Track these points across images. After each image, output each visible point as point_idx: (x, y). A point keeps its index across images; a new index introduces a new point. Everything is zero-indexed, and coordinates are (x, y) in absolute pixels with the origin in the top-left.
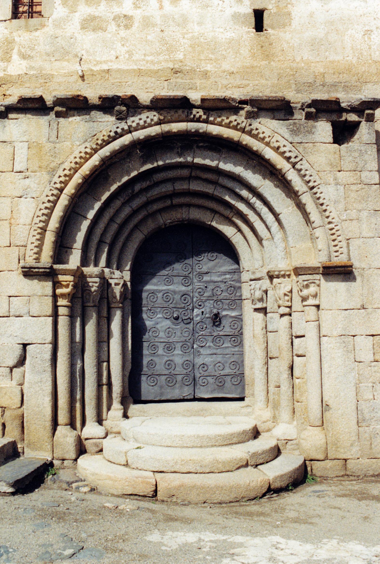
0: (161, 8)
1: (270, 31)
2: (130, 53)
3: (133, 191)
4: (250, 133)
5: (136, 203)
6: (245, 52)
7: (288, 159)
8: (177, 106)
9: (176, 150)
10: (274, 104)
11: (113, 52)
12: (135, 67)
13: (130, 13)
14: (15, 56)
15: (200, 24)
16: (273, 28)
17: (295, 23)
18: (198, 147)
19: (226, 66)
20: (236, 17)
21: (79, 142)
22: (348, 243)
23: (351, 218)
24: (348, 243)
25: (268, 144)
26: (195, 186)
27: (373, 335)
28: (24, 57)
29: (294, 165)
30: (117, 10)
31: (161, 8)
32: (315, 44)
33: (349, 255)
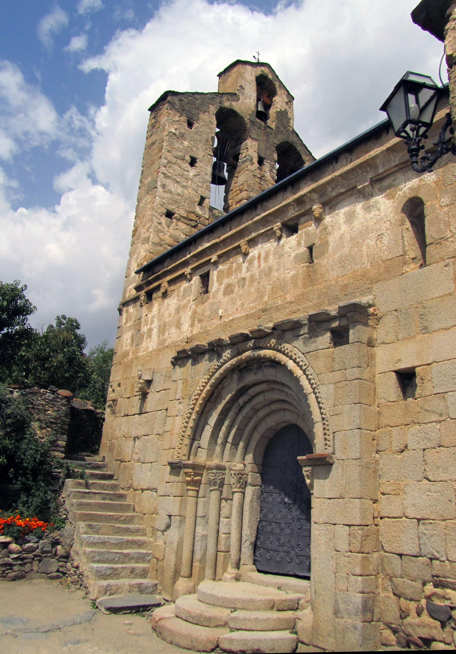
0: (259, 266)
1: (315, 261)
2: (242, 304)
3: (239, 404)
4: (280, 351)
5: (244, 412)
6: (300, 283)
7: (301, 367)
8: (238, 342)
9: (254, 371)
10: (289, 326)
11: (235, 307)
12: (244, 314)
13: (245, 276)
14: (196, 322)
15: (278, 270)
16: (317, 259)
17: (330, 248)
18: (265, 366)
19: (289, 298)
21: (202, 375)
22: (334, 436)
23: (336, 413)
24: (334, 436)
25: (291, 358)
26: (276, 396)
27: (349, 526)
28: (200, 321)
29: (304, 372)
31: (259, 266)
32: (343, 262)
33: (334, 448)
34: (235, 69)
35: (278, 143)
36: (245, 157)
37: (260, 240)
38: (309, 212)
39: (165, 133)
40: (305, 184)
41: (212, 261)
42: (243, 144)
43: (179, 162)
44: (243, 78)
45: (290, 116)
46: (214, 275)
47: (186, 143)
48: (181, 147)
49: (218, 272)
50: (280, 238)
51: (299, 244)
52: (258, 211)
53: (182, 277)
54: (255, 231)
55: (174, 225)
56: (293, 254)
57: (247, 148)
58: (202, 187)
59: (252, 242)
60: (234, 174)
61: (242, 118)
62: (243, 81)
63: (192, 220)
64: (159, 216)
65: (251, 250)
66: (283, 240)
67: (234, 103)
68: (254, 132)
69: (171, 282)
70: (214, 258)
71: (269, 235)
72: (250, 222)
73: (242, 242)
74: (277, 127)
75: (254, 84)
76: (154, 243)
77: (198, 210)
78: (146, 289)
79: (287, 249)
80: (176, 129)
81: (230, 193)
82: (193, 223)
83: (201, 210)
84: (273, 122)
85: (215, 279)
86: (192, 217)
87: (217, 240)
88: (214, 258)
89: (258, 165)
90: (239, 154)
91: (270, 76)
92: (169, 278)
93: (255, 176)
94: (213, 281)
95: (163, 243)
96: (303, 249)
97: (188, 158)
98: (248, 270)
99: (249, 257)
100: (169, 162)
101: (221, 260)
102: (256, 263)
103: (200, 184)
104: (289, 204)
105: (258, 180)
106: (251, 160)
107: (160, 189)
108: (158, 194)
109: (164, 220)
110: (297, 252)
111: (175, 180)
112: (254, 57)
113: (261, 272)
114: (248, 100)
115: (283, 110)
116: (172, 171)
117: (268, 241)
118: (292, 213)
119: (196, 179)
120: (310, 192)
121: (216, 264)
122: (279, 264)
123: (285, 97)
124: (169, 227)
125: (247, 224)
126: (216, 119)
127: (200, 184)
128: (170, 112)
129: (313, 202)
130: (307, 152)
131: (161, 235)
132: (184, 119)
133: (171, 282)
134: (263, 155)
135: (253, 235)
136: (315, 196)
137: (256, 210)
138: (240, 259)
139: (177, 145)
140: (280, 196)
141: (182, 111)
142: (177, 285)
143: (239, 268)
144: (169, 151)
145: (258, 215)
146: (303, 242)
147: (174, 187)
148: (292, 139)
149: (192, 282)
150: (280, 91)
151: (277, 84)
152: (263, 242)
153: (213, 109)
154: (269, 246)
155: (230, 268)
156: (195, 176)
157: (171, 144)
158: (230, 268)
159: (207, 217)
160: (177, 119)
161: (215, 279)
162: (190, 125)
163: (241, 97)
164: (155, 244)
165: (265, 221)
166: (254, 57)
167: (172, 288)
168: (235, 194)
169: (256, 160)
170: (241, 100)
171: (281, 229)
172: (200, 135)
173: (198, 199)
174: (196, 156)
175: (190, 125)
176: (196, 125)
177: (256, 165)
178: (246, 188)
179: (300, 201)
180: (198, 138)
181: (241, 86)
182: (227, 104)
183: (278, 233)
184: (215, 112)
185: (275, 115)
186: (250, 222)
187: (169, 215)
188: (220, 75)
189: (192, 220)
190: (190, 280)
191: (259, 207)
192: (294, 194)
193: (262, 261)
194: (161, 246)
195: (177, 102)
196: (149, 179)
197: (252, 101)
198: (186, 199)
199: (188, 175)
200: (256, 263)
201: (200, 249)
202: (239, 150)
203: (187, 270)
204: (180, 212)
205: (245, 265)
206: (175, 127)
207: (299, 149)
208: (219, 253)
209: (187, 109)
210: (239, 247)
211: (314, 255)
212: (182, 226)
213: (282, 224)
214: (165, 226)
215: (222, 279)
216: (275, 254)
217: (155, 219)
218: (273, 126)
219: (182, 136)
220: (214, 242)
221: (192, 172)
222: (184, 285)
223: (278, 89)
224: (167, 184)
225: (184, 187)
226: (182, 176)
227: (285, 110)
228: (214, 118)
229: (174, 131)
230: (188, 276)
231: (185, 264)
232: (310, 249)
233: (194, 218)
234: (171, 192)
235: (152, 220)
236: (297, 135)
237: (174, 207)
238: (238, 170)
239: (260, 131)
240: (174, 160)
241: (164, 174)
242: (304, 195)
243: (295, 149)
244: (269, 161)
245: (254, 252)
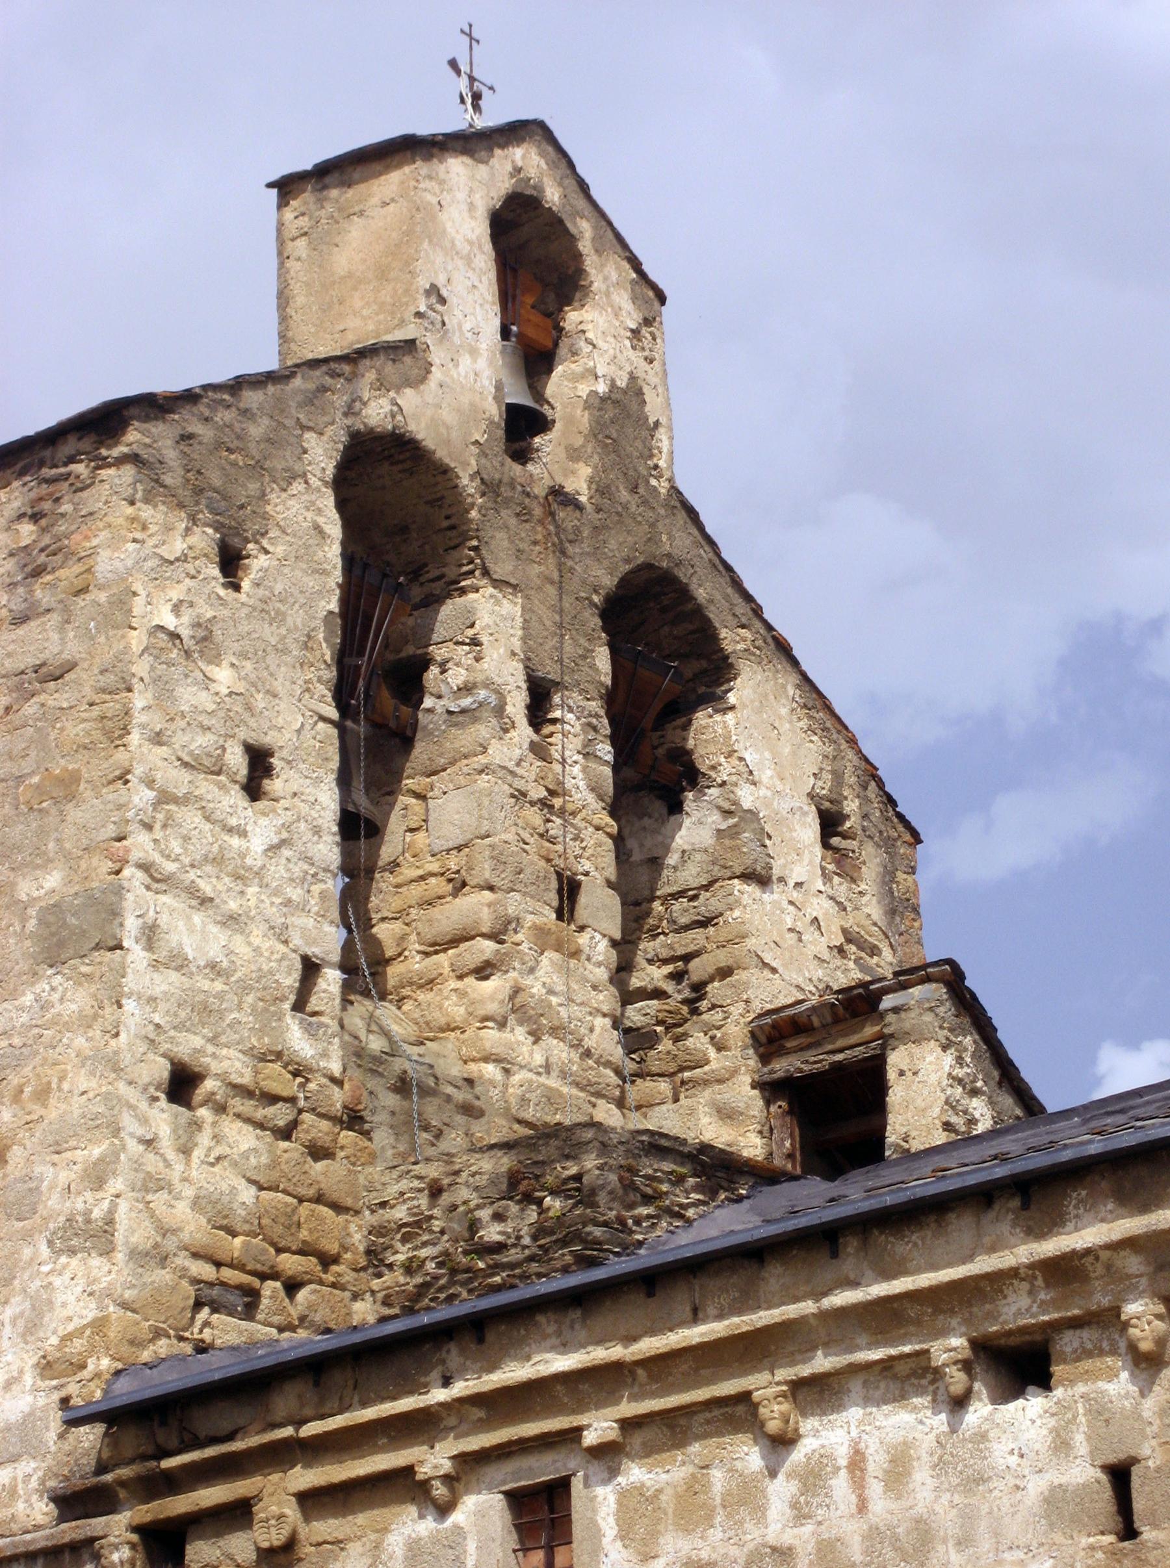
0: (862, 1506)
1: (1148, 1534)
13: (787, 1538)
16: (1155, 1526)
20: (1054, 1500)
30: (753, 1535)
31: (862, 1506)
34: (391, 182)
35: (609, 582)
36: (467, 689)
37: (856, 1386)
38: (1108, 1320)
39: (137, 640)
40: (1090, 1205)
41: (590, 1438)
42: (448, 609)
43: (205, 787)
44: (436, 236)
45: (653, 408)
46: (598, 1504)
47: (223, 676)
48: (205, 700)
49: (623, 1495)
50: (959, 1403)
51: (1061, 1445)
52: (848, 1265)
53: (402, 1485)
54: (829, 1345)
55: (204, 1139)
56: (1036, 1486)
57: (475, 642)
58: (303, 908)
59: (817, 1393)
60: (398, 776)
61: (445, 471)
62: (439, 258)
63: (272, 1099)
64: (143, 1105)
65: (808, 1425)
66: (979, 1411)
67: (409, 399)
68: (502, 541)
69: (313, 1501)
70: (599, 1427)
71: (907, 1377)
72: (808, 1307)
73: (765, 1385)
74: (602, 490)
75: (485, 260)
76: (139, 1256)
77: (297, 1040)
78: (146, 1512)
79: (1000, 1452)
80: (176, 609)
81: (383, 882)
82: (280, 1115)
83: (310, 1031)
84: (574, 455)
85: (608, 1525)
86: (277, 1079)
87: (616, 1352)
88: (599, 1427)
89: (529, 731)
90: (425, 663)
91: (553, 195)
92: (304, 1477)
93: (520, 795)
94: (597, 1534)
95: (171, 1244)
96: (1083, 1472)
97: (237, 760)
98: (800, 1514)
99: (798, 1455)
100: (165, 798)
101: (637, 1440)
102: (840, 1485)
103: (295, 894)
104: (1013, 1273)
105: (534, 816)
106: (500, 710)
107: (137, 955)
108: (130, 982)
109: (164, 1118)
110: (1054, 1477)
111: (192, 891)
112: (453, 64)
113: (873, 1535)
114: (465, 361)
115: (622, 383)
116: (176, 846)
117: (900, 1397)
118: (1020, 1311)
119: (277, 871)
120: (1114, 1247)
121: (608, 1455)
122: (968, 1517)
123: (623, 299)
124: (186, 1151)
125: (792, 1311)
126: (341, 505)
127: (295, 894)
128: (146, 512)
129: (1125, 1286)
130: (742, 608)
131: (159, 1199)
132: (205, 539)
133: (313, 1501)
134: (549, 670)
135: (822, 1362)
136: (1133, 1263)
137: (835, 1254)
138: (750, 1456)
139: (190, 696)
140: (961, 1226)
141: (194, 496)
142: (361, 1519)
143: (747, 1498)
144: (158, 739)
145: (854, 1284)
146: (1080, 1442)
147: (191, 930)
148: (675, 542)
149: (458, 1517)
150: (604, 274)
151: (584, 230)
152: (867, 1401)
153: (322, 455)
154: (912, 1422)
155: (695, 1487)
156: (273, 849)
157: (164, 692)
158: (695, 1487)
159: (335, 1068)
160: (178, 546)
161: (608, 1525)
162: (231, 562)
163: (437, 356)
164: (139, 1256)
165: (884, 1317)
166: (453, 64)
167: (326, 1527)
168: (416, 892)
169: (517, 704)
170: (436, 374)
171: (966, 1366)
172: (279, 618)
173: (291, 980)
174: (269, 740)
175: (231, 562)
176: (257, 564)
177: (524, 732)
178: (485, 871)
179: (1063, 1271)
180: (270, 633)
181: (433, 291)
182: (377, 413)
183: (957, 1379)
184: (330, 471)
185: (584, 420)
186: (808, 1307)
187: (182, 1084)
188: (287, 187)
189: (272, 1099)
190: (444, 1510)
191: (851, 1245)
192: (1038, 1232)
193: (875, 1488)
194: (163, 1260)
195: (171, 454)
196: (53, 880)
197: (482, 364)
198: (244, 988)
199: (243, 855)
200: (840, 1485)
201: (513, 1373)
202: (424, 636)
203: (434, 1459)
204: (226, 1064)
205: (781, 1492)
206: (176, 593)
207: (701, 594)
208: (629, 1408)
209: (216, 479)
210: (744, 1397)
211: (1139, 1504)
212: (243, 1139)
213: (975, 1344)
214: (171, 1155)
215: (654, 1535)
216: (940, 1466)
217: (129, 1123)
218: (579, 483)
219: (204, 643)
220: (599, 1354)
221: (260, 828)
222: (409, 1526)
223: (591, 262)
224: (164, 920)
225: (231, 921)
226: (218, 860)
227: (633, 378)
228: (328, 501)
229: (169, 621)
230: (439, 1491)
231: (421, 1426)
232: (1120, 1476)
233: (285, 1085)
234: (178, 962)
235: (116, 1132)
236: (692, 514)
237: (197, 1041)
238: (421, 751)
239: (524, 530)
240: (179, 780)
241: (146, 867)
242: (1088, 1252)
243: (684, 593)
244: (575, 698)
245: (827, 1436)
